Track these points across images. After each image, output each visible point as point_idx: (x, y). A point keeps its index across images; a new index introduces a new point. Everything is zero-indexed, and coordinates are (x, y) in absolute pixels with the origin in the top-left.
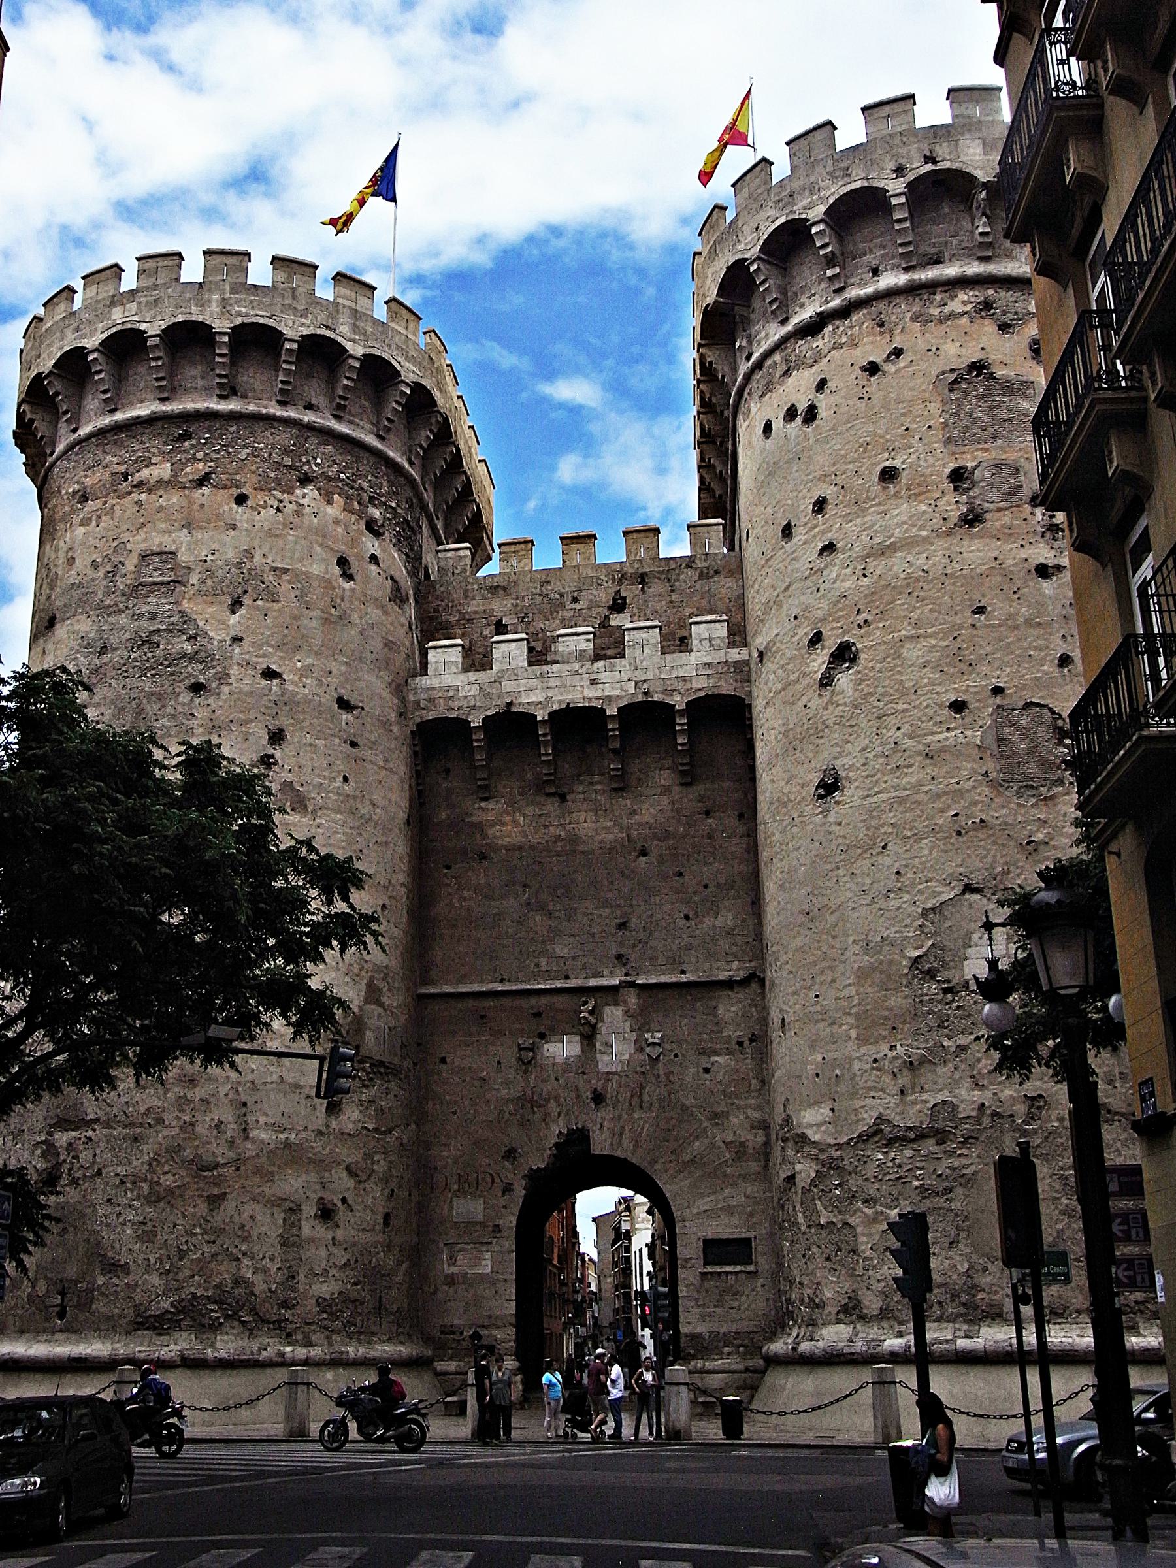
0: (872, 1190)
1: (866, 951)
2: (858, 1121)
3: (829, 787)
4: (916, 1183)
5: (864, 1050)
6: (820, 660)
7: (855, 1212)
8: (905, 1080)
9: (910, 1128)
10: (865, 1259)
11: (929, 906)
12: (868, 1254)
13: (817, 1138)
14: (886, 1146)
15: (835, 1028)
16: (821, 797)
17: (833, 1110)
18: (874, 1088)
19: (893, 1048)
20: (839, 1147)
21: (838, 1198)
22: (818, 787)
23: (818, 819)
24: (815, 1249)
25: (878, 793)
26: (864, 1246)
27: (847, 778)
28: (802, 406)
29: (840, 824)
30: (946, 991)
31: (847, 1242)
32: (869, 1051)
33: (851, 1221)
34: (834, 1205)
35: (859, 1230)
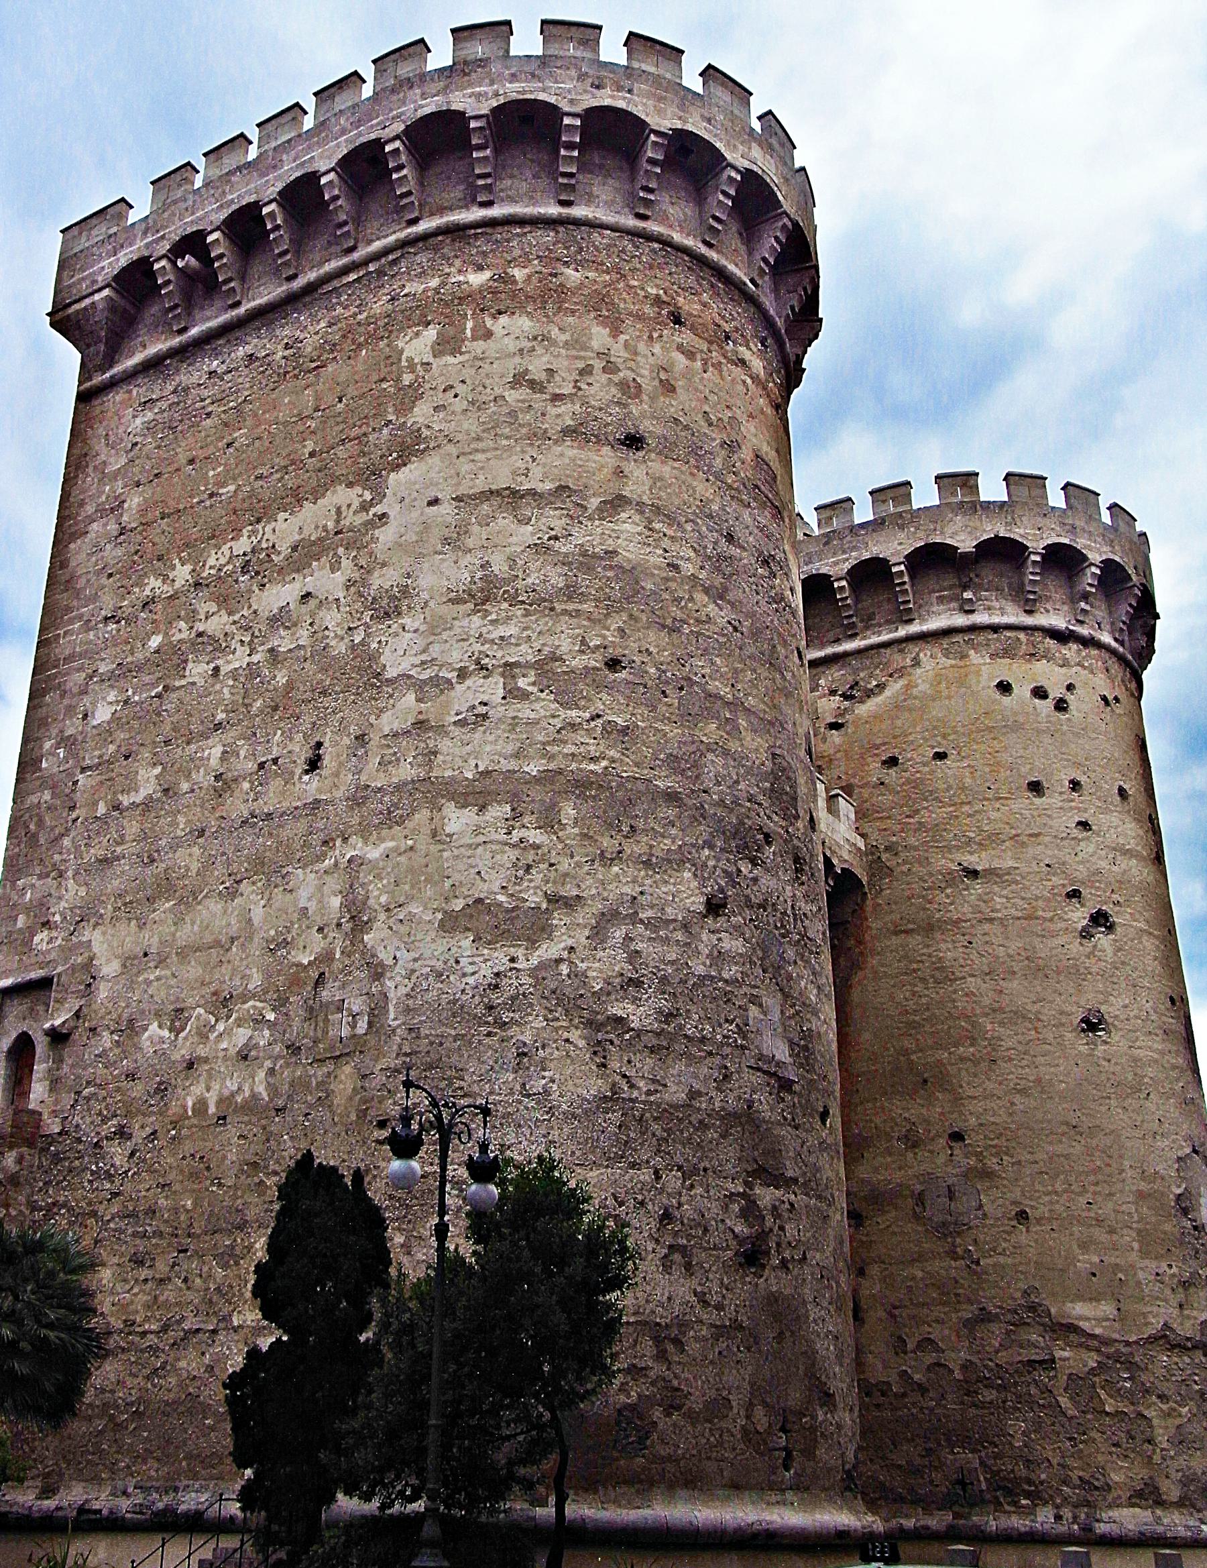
0: (1165, 1388)
1: (1143, 1179)
2: (1146, 1324)
3: (1092, 1025)
4: (1197, 1387)
5: (1147, 1262)
6: (1079, 914)
7: (1149, 1407)
8: (1181, 1296)
9: (1188, 1339)
10: (1162, 1450)
11: (1180, 1154)
12: (1165, 1445)
13: (1098, 1331)
14: (1168, 1350)
15: (1115, 1237)
16: (1083, 1030)
17: (1119, 1309)
18: (1158, 1298)
19: (1170, 1266)
20: (1128, 1344)
21: (1129, 1391)
22: (1082, 1021)
23: (1084, 1049)
24: (1094, 1434)
25: (1140, 1048)
26: (1162, 1439)
27: (1115, 1026)
28: (1056, 692)
29: (1109, 1061)
30: (1195, 1228)
31: (1143, 1432)
32: (1152, 1265)
33: (1146, 1413)
34: (1118, 1393)
35: (1155, 1422)
